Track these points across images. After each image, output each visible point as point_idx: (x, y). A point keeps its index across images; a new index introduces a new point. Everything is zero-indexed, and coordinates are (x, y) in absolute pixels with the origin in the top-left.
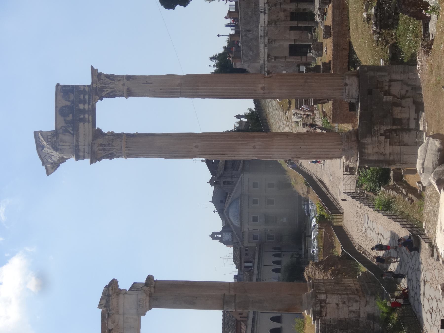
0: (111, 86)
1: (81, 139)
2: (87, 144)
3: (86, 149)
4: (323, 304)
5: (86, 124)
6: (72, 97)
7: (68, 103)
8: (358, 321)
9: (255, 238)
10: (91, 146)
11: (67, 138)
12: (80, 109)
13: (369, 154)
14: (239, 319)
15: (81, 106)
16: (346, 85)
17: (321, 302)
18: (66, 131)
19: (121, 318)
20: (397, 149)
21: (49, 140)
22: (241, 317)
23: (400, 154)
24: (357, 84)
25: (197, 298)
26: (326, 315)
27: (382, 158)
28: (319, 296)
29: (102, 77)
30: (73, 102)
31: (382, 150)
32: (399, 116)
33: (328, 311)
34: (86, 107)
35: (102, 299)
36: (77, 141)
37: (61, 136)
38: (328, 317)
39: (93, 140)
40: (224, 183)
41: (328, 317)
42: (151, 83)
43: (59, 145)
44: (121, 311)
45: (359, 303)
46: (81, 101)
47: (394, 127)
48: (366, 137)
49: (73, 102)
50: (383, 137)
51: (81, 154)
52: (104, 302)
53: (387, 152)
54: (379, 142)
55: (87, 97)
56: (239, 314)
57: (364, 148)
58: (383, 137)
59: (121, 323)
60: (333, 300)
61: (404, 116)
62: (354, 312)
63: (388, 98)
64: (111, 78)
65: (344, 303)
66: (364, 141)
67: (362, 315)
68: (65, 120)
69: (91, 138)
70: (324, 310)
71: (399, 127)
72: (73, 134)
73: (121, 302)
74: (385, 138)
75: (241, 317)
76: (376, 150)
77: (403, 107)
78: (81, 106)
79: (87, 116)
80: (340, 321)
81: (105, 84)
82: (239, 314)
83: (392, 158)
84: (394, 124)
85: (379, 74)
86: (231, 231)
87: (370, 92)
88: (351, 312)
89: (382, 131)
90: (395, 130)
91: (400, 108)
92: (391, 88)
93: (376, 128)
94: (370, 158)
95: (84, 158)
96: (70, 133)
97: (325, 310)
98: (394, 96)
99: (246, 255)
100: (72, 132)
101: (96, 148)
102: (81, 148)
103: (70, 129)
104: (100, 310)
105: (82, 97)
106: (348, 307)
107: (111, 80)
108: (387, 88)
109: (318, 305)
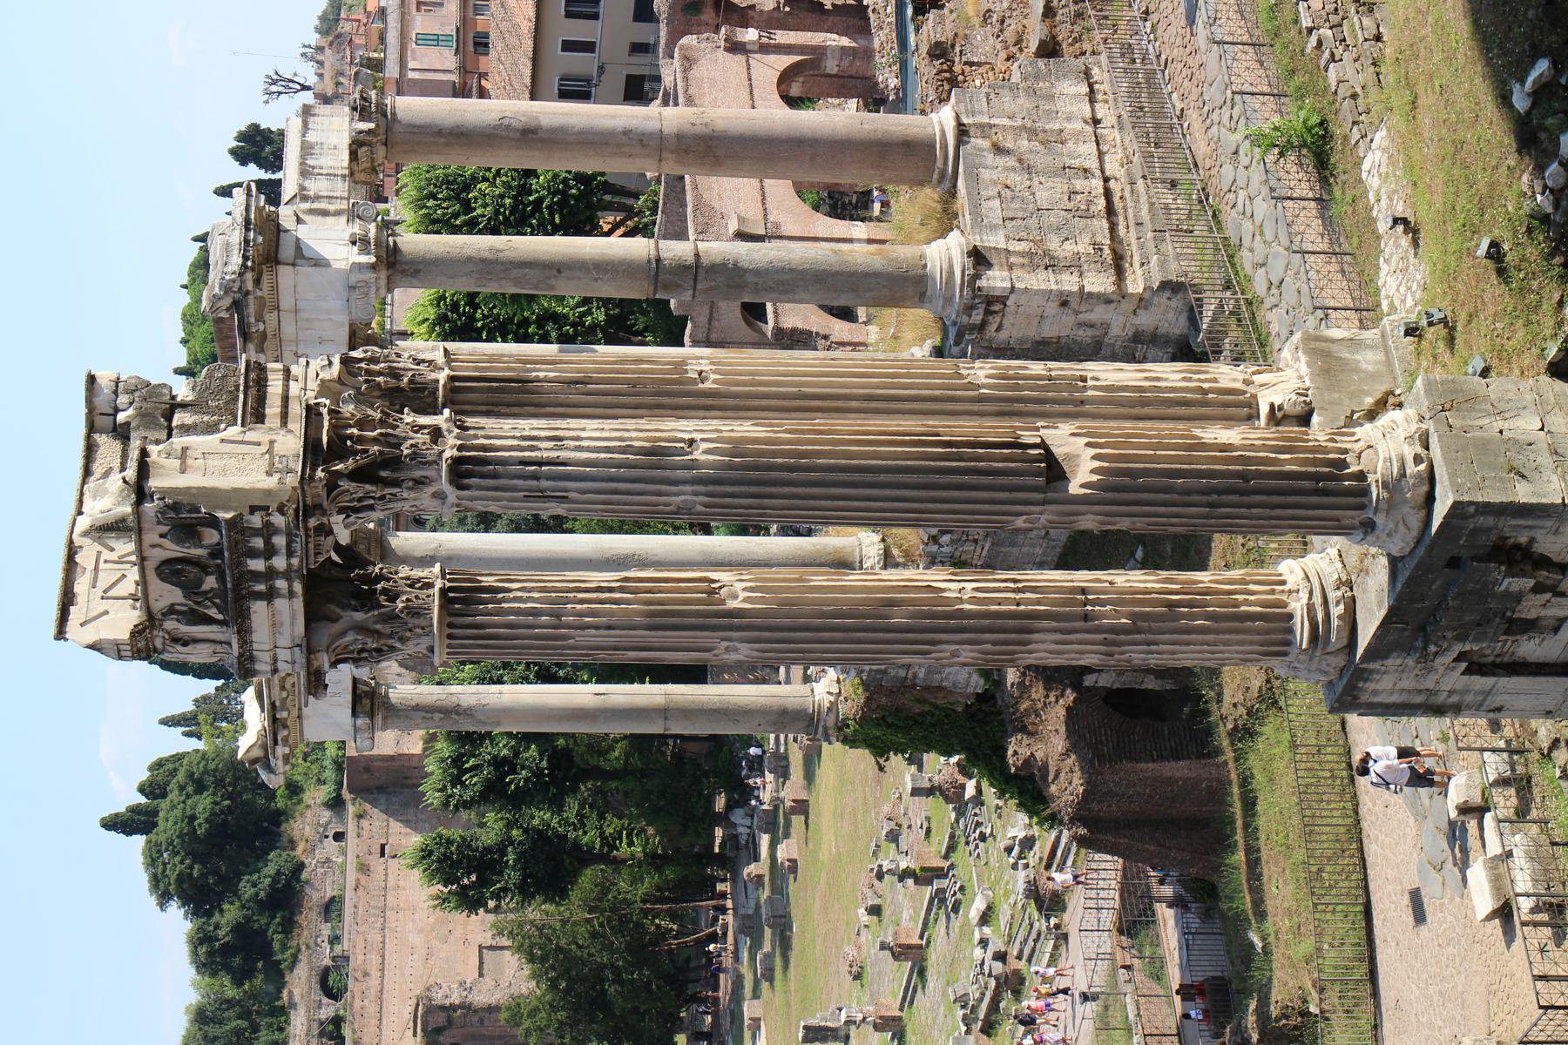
2: (284, 641)
4: (996, 307)
5: (280, 603)
12: (252, 572)
13: (1375, 693)
15: (257, 565)
23: (1488, 693)
25: (559, 271)
26: (998, 329)
33: (1006, 323)
38: (1003, 335)
41: (1003, 335)
45: (1113, 305)
46: (254, 554)
48: (1386, 657)
57: (1366, 680)
62: (1092, 326)
67: (1115, 331)
69: (300, 629)
70: (994, 321)
76: (1407, 683)
78: (257, 565)
79: (281, 584)
83: (1454, 699)
88: (1081, 325)
91: (1548, 596)
94: (1377, 700)
97: (998, 319)
100: (220, 617)
106: (1077, 313)
107: (386, 483)
109: (981, 311)
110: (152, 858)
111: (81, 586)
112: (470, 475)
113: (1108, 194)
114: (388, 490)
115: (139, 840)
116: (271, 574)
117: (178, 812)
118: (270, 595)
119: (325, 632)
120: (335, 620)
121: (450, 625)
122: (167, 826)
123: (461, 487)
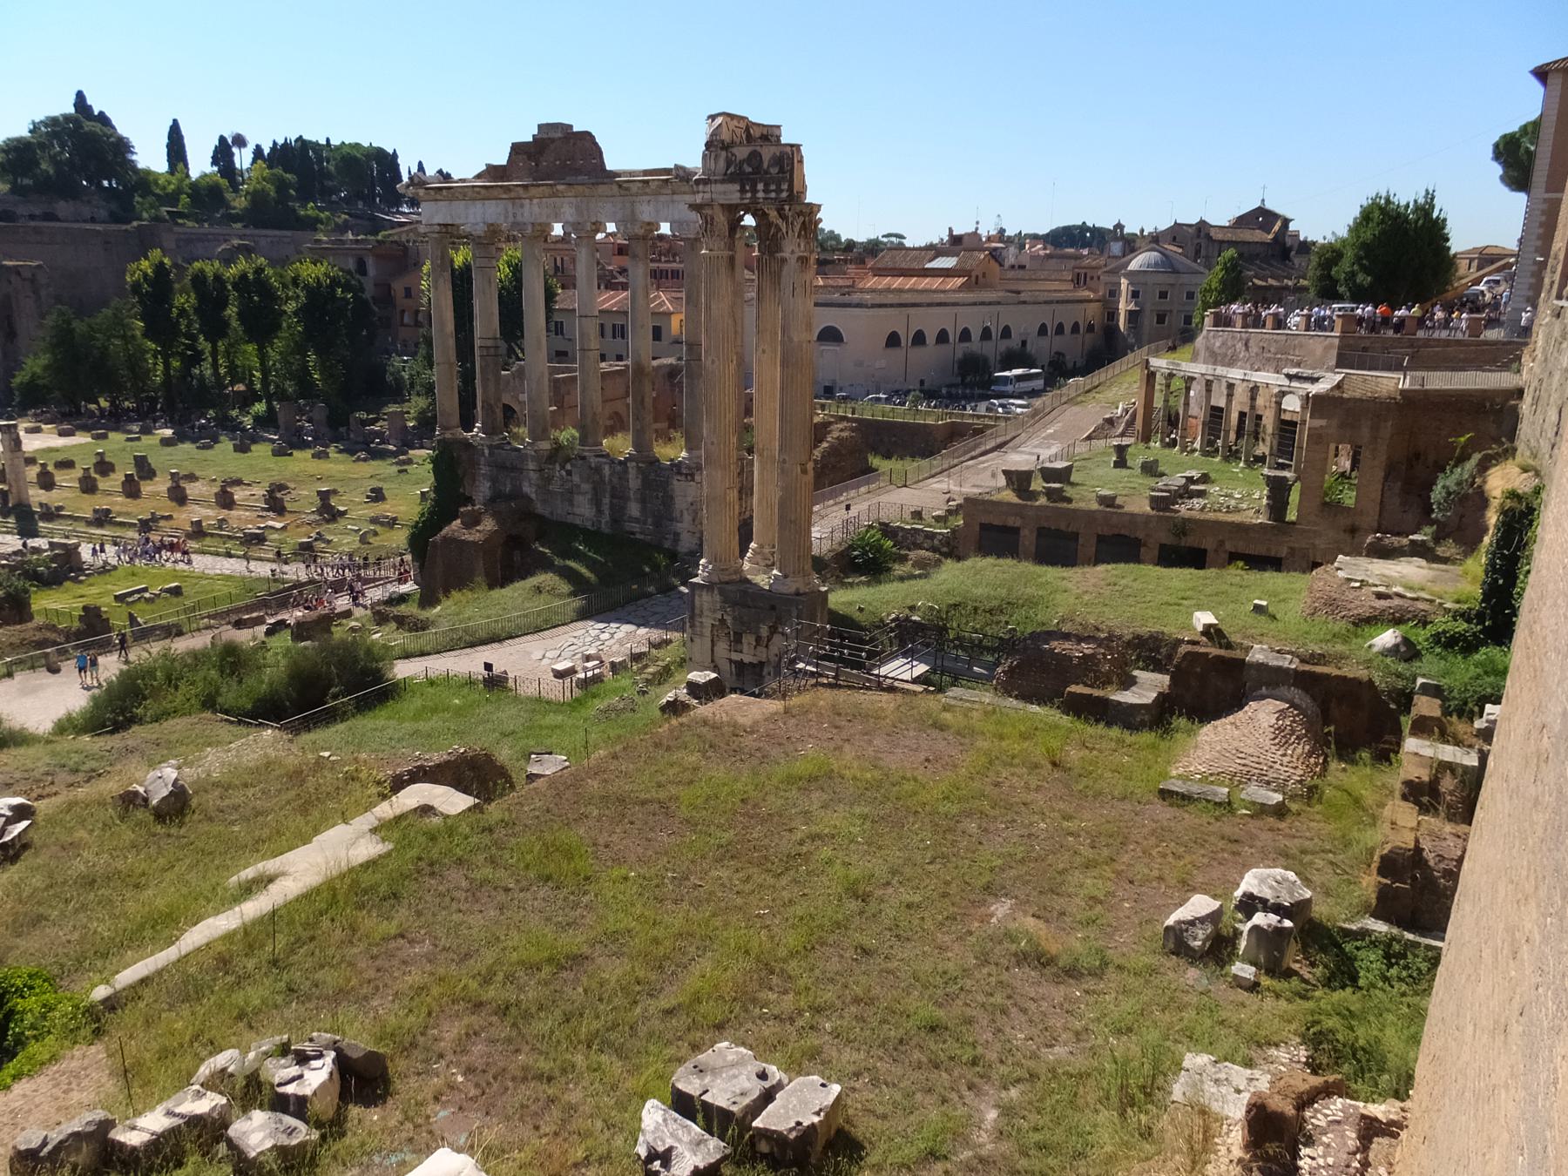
1: (720, 187)
3: (707, 196)
6: (774, 171)
7: (765, 165)
8: (672, 520)
10: (710, 205)
11: (722, 164)
15: (760, 186)
17: (692, 475)
18: (729, 164)
20: (707, 632)
23: (702, 635)
30: (767, 172)
31: (706, 613)
34: (761, 195)
35: (683, 168)
37: (724, 153)
40: (1199, 245)
44: (676, 197)
49: (767, 172)
54: (714, 611)
55: (773, 195)
59: (662, 198)
61: (745, 648)
63: (764, 631)
76: (706, 606)
78: (760, 186)
80: (672, 498)
87: (773, 608)
101: (708, 211)
102: (708, 188)
103: (732, 169)
110: (67, 118)
111: (735, 122)
115: (72, 110)
116: (754, 191)
118: (743, 191)
122: (88, 126)
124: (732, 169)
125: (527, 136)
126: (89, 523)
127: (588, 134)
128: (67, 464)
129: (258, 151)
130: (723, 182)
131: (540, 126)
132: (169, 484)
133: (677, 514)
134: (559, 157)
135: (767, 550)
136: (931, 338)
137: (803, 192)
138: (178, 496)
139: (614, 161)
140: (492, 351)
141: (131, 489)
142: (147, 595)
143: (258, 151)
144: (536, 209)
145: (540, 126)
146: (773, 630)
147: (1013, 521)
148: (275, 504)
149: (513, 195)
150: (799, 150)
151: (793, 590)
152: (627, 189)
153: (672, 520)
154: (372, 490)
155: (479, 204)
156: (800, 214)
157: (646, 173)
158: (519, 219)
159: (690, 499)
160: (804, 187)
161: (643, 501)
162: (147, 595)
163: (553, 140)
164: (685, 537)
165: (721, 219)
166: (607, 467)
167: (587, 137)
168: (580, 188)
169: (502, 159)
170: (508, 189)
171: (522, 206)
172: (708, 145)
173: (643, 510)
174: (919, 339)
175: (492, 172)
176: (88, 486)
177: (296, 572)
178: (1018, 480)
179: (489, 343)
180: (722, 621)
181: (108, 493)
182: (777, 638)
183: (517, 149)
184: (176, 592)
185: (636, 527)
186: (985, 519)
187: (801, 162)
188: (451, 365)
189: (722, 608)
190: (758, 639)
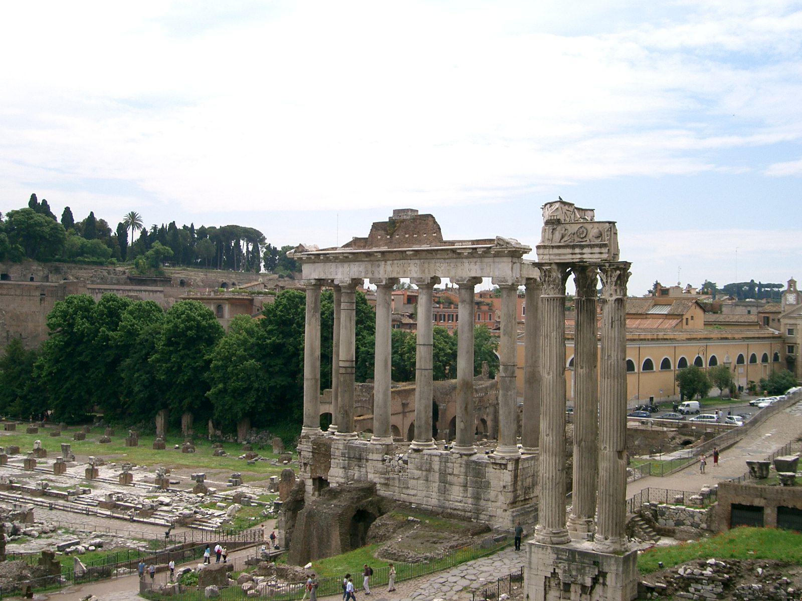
0: (609, 281)
1: (556, 251)
2: (552, 257)
4: (503, 467)
5: (570, 256)
7: (591, 236)
8: (488, 500)
9: (791, 331)
11: (557, 235)
14: (684, 317)
16: (606, 539)
17: (506, 465)
19: (491, 260)
21: (552, 218)
22: (687, 319)
24: (606, 550)
27: (533, 566)
28: (510, 462)
29: (618, 272)
32: (573, 588)
35: (503, 240)
36: (553, 247)
39: (556, 263)
41: (491, 470)
42: (612, 327)
43: (549, 227)
44: (497, 259)
47: (561, 584)
50: (553, 571)
51: (541, 251)
52: (501, 243)
53: (539, 573)
56: (692, 317)
57: (543, 549)
58: (553, 571)
59: (486, 260)
60: (507, 476)
63: (588, 582)
64: (619, 282)
65: (504, 487)
66: (549, 550)
68: (574, 234)
71: (562, 588)
72: (560, 242)
73: (505, 259)
74: (551, 573)
75: (687, 319)
77: (581, 595)
81: (611, 276)
82: (692, 317)
84: (565, 584)
85: (614, 575)
86: (798, 304)
87: (596, 563)
89: (557, 571)
90: (559, 584)
91: (580, 592)
92: (602, 586)
93: (560, 565)
94: (533, 554)
95: (538, 255)
96: (561, 240)
98: (592, 588)
99: (773, 320)
100: (562, 241)
102: (546, 251)
104: (494, 238)
105: (597, 250)
108: (601, 581)
110: (24, 211)
111: (567, 207)
112: (618, 304)
113: (529, 499)
114: (614, 283)
117: (43, 220)
119: (554, 267)
120: (558, 270)
121: (554, 300)
122: (39, 217)
123: (615, 300)
124: (564, 240)
125: (385, 217)
126: (33, 493)
127: (431, 216)
128: (15, 451)
129: (144, 232)
130: (559, 247)
131: (394, 211)
132: (86, 466)
133: (492, 494)
134: (405, 232)
135: (584, 519)
136: (657, 366)
137: (616, 255)
138: (92, 473)
139: (447, 235)
140: (349, 370)
141: (59, 468)
142: (80, 547)
143: (144, 232)
144: (389, 268)
145: (394, 211)
146: (595, 580)
147: (758, 502)
148: (162, 484)
149: (372, 258)
150: (615, 226)
151: (611, 549)
152: (459, 254)
153: (488, 500)
154: (234, 476)
155: (346, 265)
156: (618, 268)
157: (473, 242)
158: (377, 276)
159: (502, 484)
160: (618, 250)
161: (465, 486)
162: (80, 547)
163: (403, 221)
164: (499, 512)
165: (557, 274)
166: (437, 459)
167: (429, 219)
168: (424, 253)
169: (365, 233)
170: (368, 254)
171: (379, 266)
172: (547, 223)
173: (466, 491)
174: (648, 365)
175: (356, 242)
176: (30, 464)
177: (182, 535)
178: (759, 470)
179: (347, 364)
180: (554, 574)
181: (43, 472)
182: (598, 589)
183: (376, 226)
184: (99, 545)
185: (459, 505)
186: (738, 500)
187: (616, 234)
188: (316, 381)
189: (556, 564)
190: (584, 587)
